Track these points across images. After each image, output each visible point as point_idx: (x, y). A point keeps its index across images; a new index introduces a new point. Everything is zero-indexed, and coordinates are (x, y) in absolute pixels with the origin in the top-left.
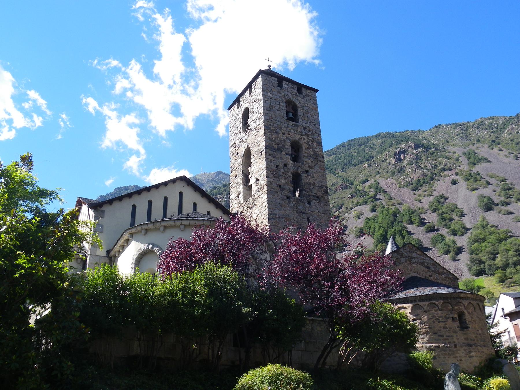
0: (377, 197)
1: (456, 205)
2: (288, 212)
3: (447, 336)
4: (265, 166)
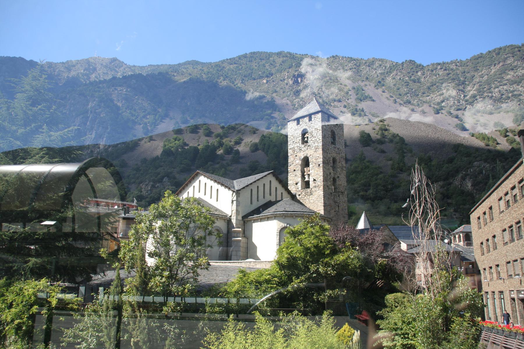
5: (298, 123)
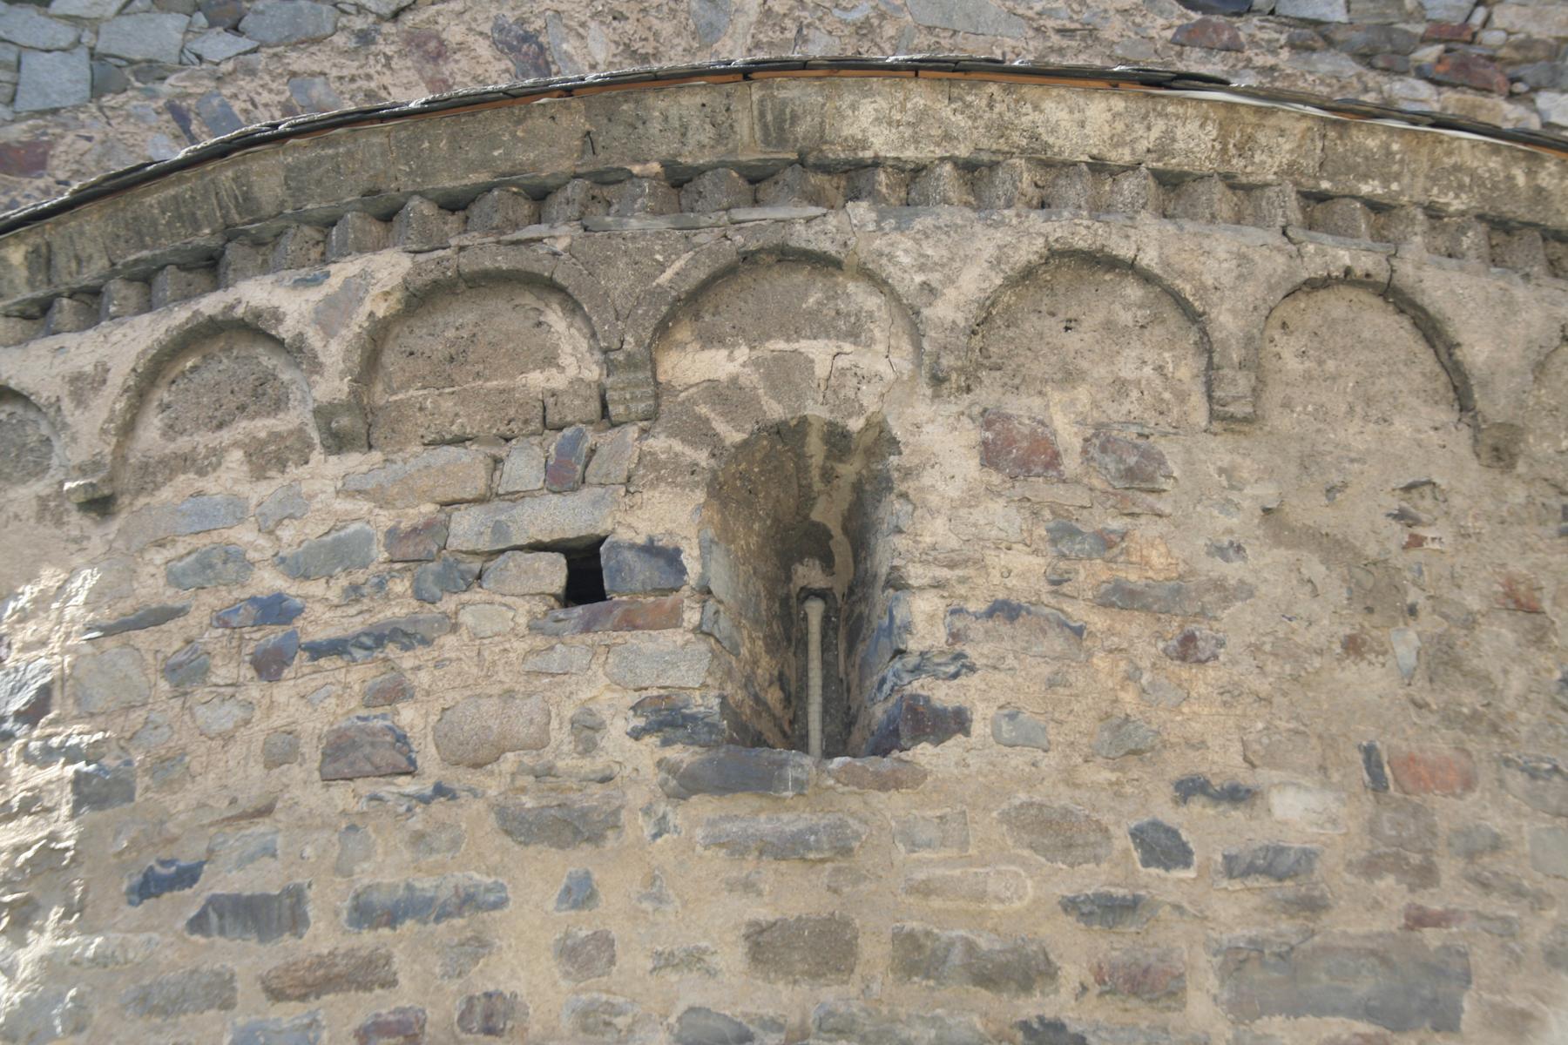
3: (364, 913)
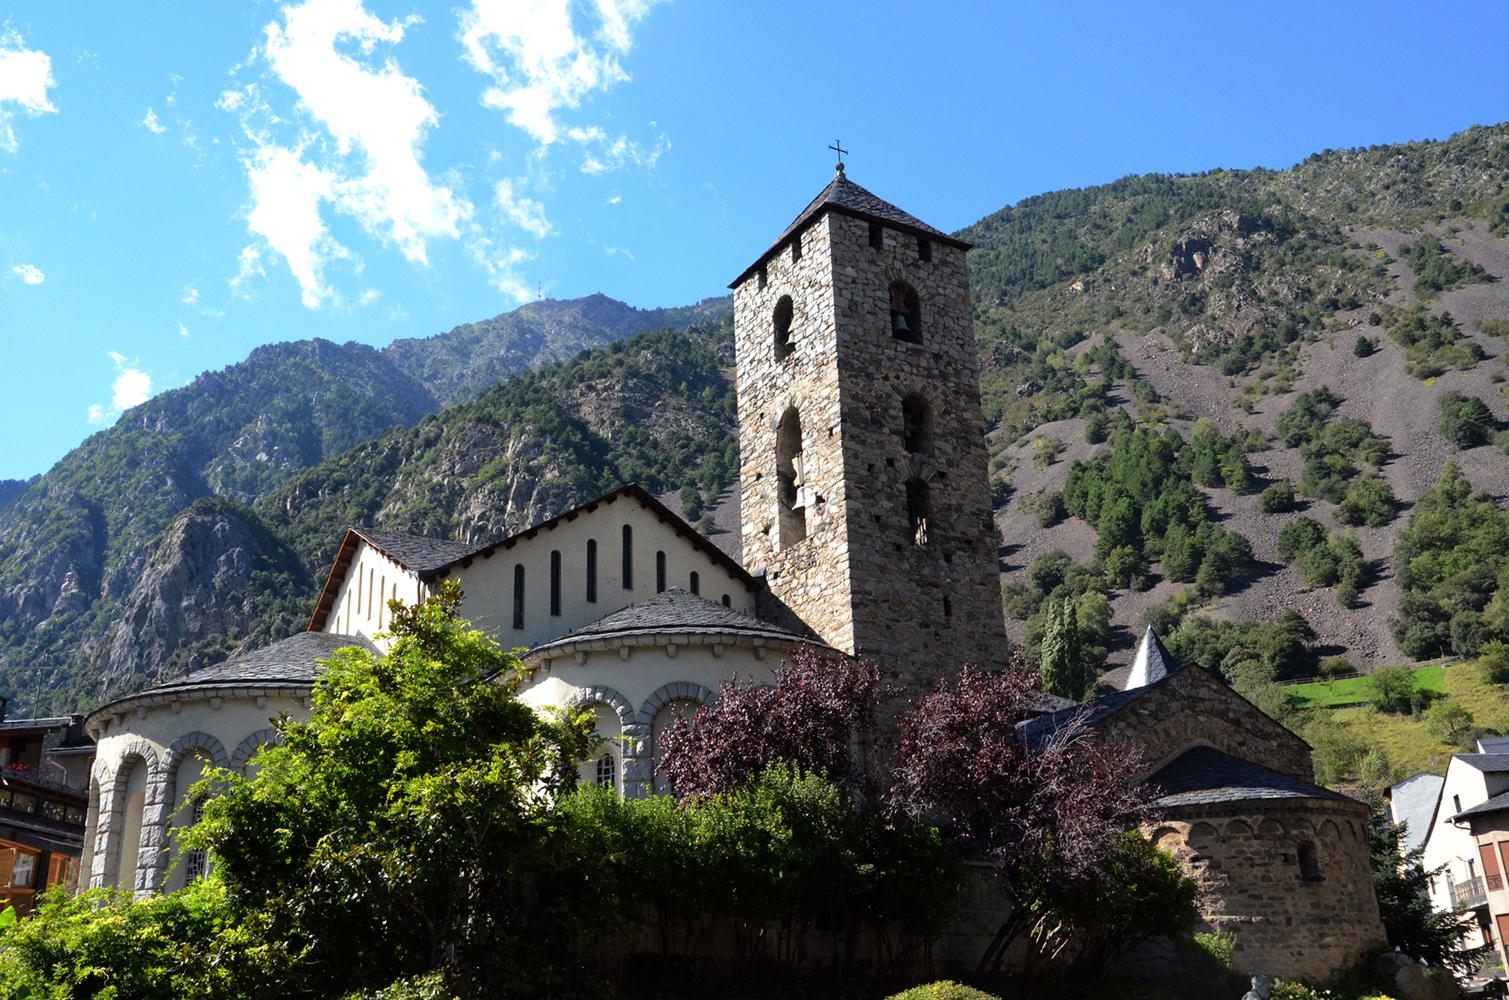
0: (1110, 394)
1: (1367, 425)
2: (898, 585)
3: (1270, 898)
4: (840, 468)
5: (763, 282)
